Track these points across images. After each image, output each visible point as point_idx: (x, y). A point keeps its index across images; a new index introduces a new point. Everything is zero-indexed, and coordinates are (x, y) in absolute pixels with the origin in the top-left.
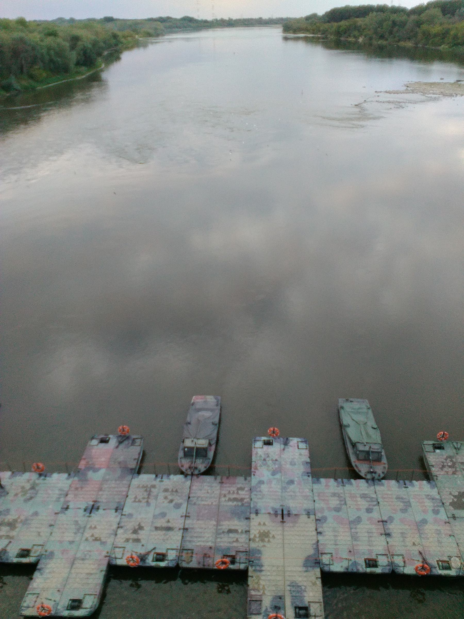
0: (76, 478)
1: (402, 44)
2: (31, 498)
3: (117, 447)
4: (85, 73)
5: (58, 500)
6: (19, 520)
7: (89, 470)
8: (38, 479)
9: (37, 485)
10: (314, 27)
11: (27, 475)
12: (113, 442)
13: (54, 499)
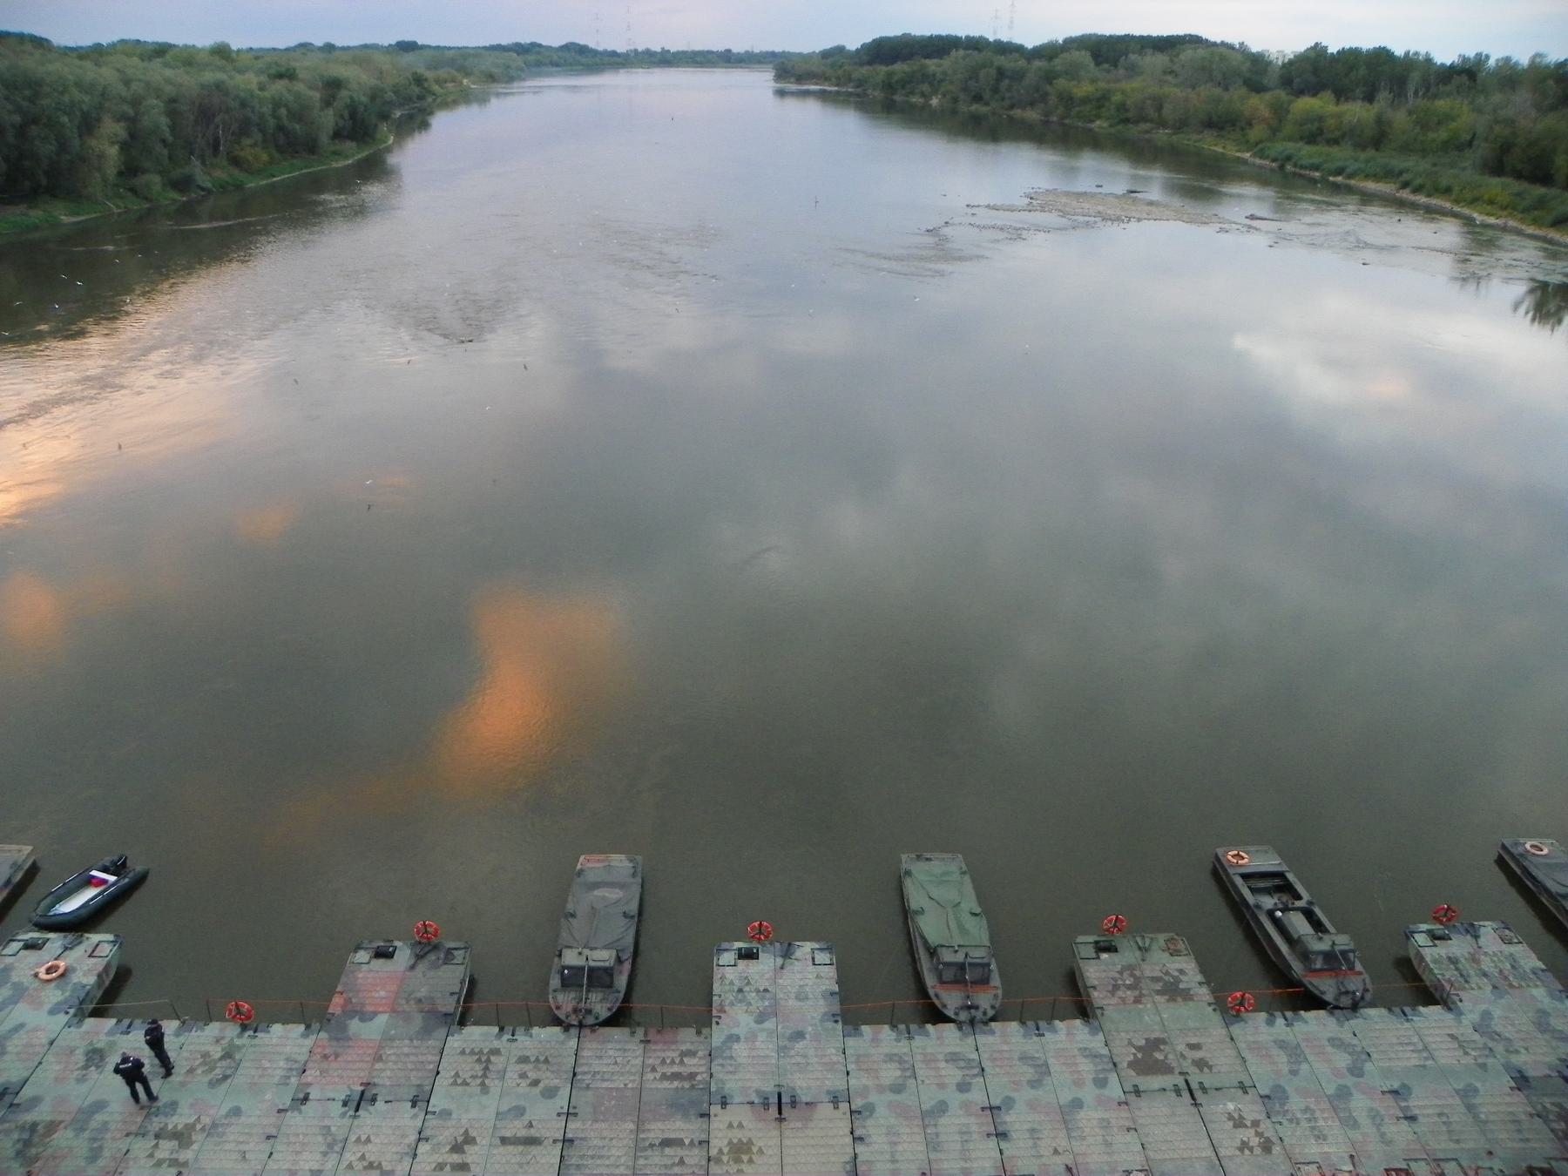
0: (323, 1035)
1: (1017, 113)
2: (226, 1077)
3: (412, 967)
4: (353, 154)
5: (284, 1081)
6: (198, 1127)
7: (352, 1018)
8: (240, 1035)
9: (239, 1048)
10: (840, 72)
11: (214, 1028)
12: (404, 955)
13: (276, 1080)
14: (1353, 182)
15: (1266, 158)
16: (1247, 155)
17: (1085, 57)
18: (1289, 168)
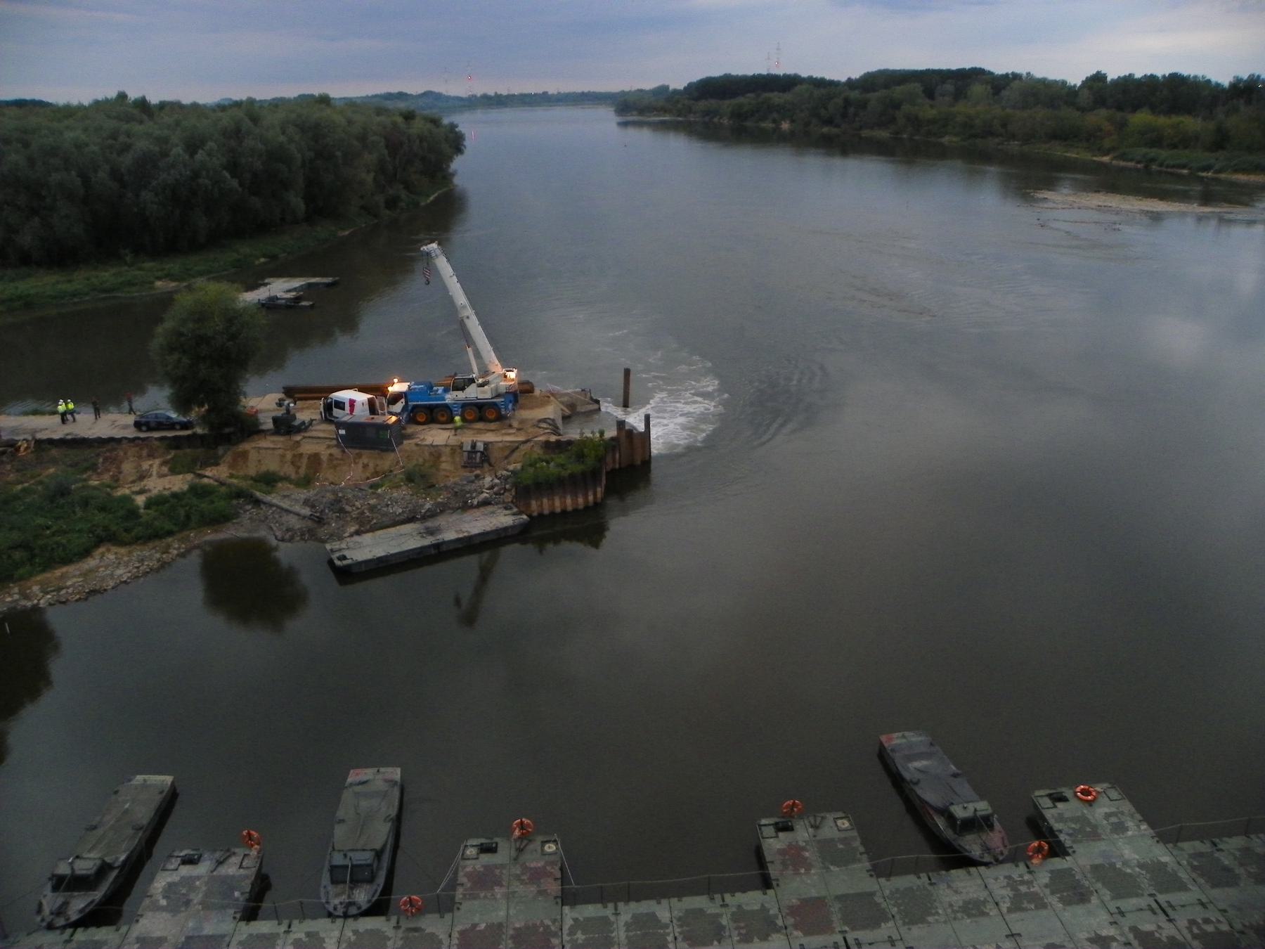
1: (866, 133)
10: (680, 106)
14: (1223, 176)
15: (1131, 160)
16: (1106, 159)
17: (917, 87)
18: (1154, 167)
